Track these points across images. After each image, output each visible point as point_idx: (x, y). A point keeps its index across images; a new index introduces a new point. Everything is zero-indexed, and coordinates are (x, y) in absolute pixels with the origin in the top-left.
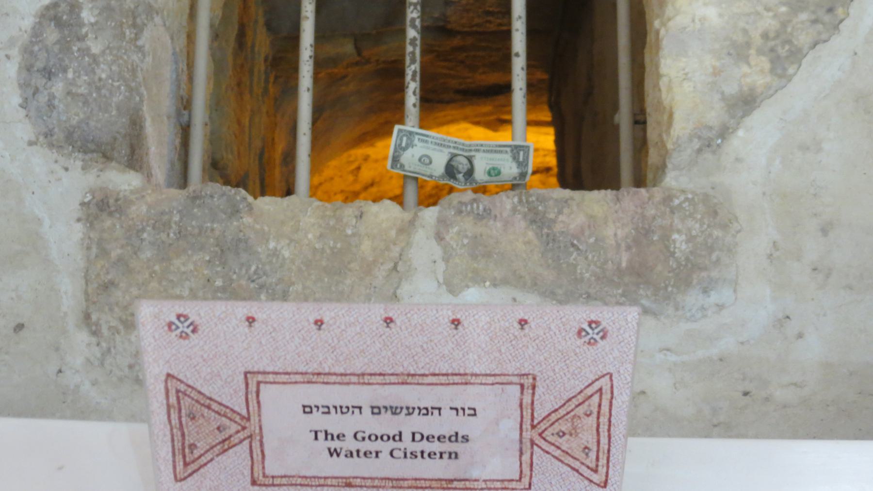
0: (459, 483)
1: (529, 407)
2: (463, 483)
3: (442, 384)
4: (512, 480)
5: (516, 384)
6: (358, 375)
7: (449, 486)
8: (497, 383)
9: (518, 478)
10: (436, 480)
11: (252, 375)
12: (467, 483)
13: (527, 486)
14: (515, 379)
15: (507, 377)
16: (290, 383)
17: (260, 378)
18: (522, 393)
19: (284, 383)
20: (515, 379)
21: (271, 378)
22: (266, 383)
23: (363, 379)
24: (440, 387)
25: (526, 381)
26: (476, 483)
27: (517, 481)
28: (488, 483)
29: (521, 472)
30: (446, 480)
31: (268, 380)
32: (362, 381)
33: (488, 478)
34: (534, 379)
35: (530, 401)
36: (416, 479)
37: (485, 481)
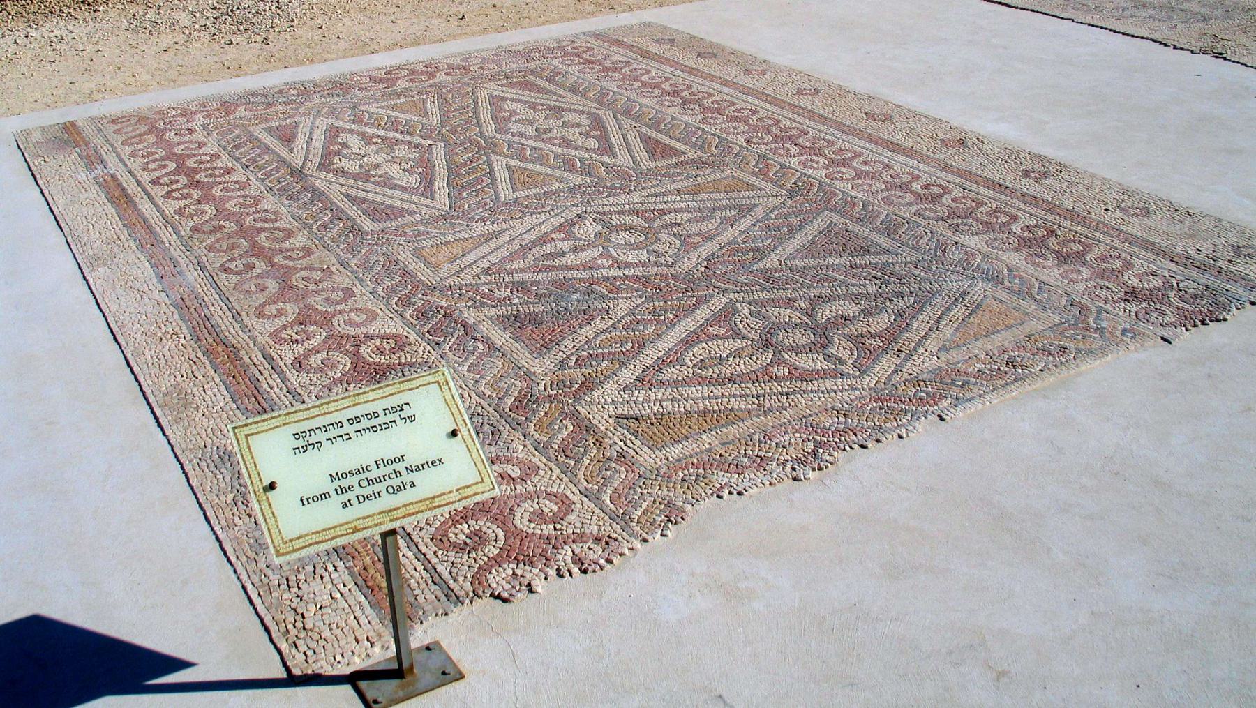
0: (439, 498)
1: (453, 403)
2: (442, 497)
3: (382, 398)
4: (477, 483)
5: (433, 383)
6: (318, 406)
7: (434, 505)
8: (420, 386)
9: (481, 480)
10: (421, 501)
11: (239, 430)
12: (445, 496)
13: (491, 487)
14: (431, 379)
15: (424, 378)
16: (271, 429)
17: (246, 430)
18: (441, 390)
19: (266, 431)
20: (431, 379)
21: (253, 429)
22: (252, 434)
23: (323, 409)
24: (381, 401)
25: (439, 378)
26: (451, 495)
27: (481, 482)
28: (460, 491)
29: (479, 471)
30: (428, 499)
31: (252, 431)
32: (323, 412)
33: (458, 487)
34: (444, 374)
35: (451, 397)
36: (405, 506)
37: (457, 490)
